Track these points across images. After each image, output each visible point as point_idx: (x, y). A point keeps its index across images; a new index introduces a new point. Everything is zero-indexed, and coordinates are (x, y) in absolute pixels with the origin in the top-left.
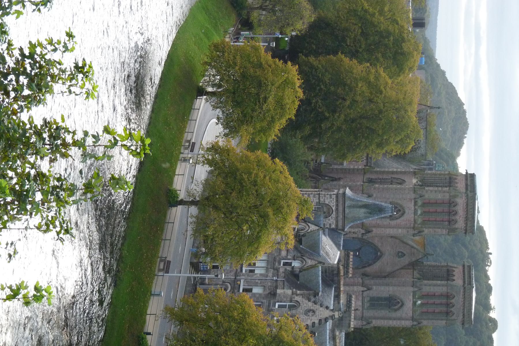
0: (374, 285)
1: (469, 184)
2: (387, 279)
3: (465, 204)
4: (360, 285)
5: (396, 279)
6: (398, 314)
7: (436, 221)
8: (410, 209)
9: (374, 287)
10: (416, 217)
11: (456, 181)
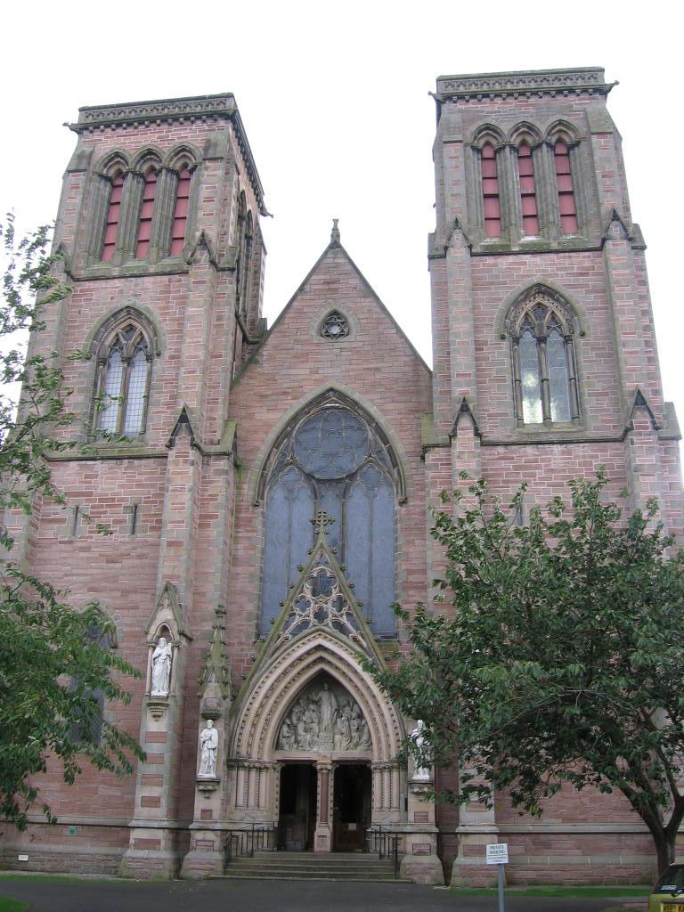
3: (120, 131)
10: (152, 270)
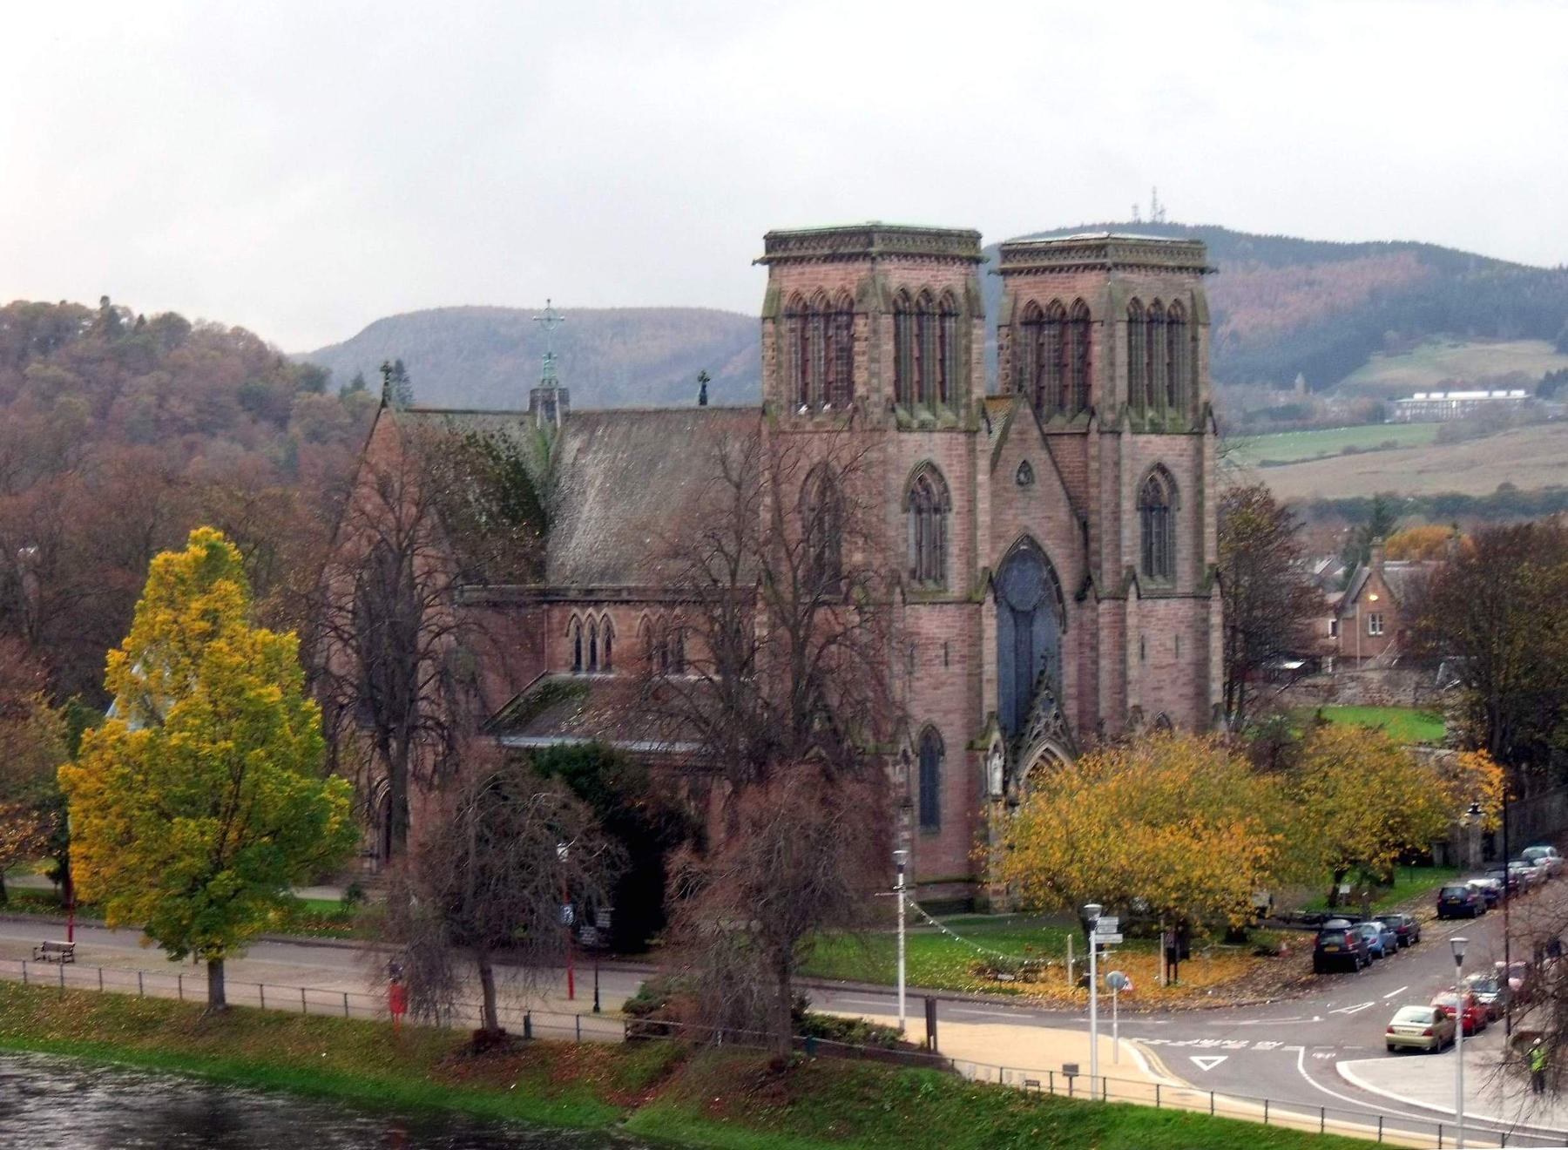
0: (1118, 560)
1: (827, 251)
2: (1093, 519)
3: (903, 261)
4: (1124, 607)
5: (1093, 491)
6: (1184, 480)
7: (942, 361)
8: (920, 445)
9: (1126, 559)
11: (807, 296)
